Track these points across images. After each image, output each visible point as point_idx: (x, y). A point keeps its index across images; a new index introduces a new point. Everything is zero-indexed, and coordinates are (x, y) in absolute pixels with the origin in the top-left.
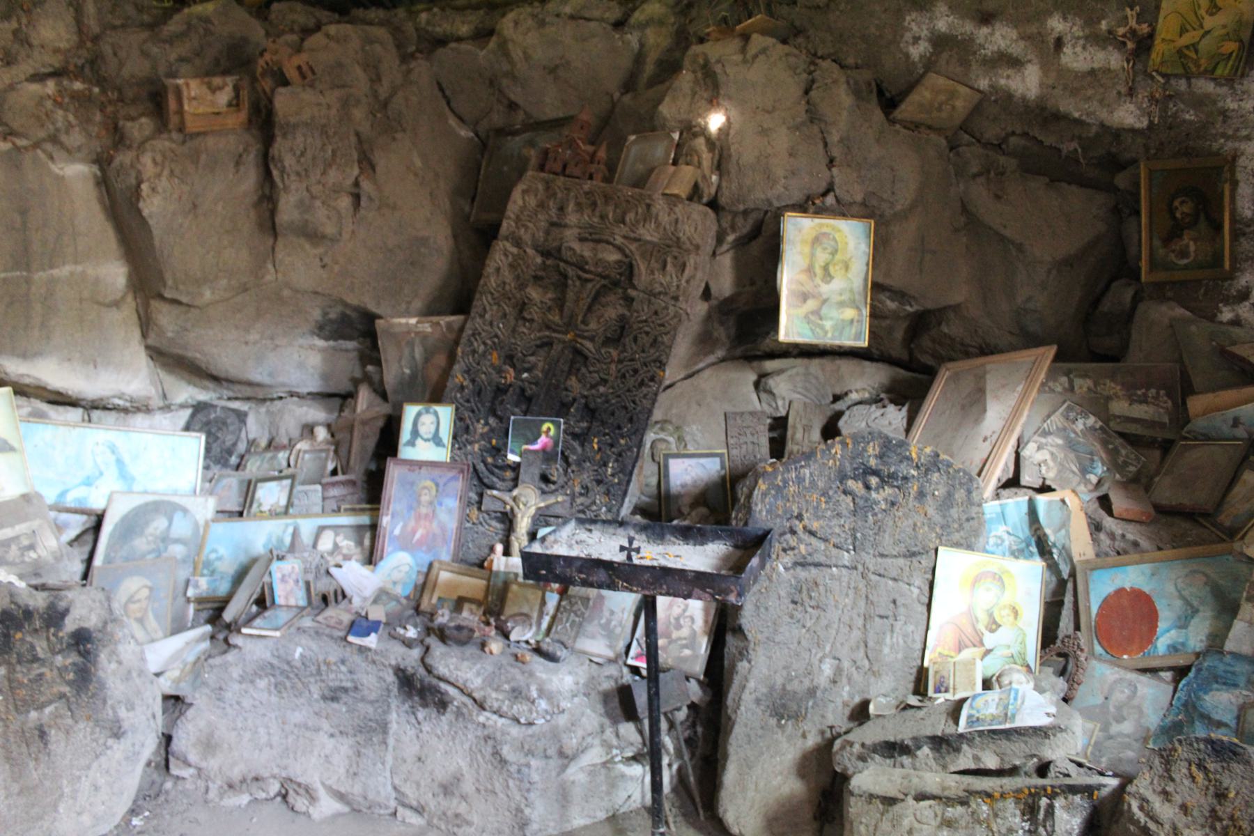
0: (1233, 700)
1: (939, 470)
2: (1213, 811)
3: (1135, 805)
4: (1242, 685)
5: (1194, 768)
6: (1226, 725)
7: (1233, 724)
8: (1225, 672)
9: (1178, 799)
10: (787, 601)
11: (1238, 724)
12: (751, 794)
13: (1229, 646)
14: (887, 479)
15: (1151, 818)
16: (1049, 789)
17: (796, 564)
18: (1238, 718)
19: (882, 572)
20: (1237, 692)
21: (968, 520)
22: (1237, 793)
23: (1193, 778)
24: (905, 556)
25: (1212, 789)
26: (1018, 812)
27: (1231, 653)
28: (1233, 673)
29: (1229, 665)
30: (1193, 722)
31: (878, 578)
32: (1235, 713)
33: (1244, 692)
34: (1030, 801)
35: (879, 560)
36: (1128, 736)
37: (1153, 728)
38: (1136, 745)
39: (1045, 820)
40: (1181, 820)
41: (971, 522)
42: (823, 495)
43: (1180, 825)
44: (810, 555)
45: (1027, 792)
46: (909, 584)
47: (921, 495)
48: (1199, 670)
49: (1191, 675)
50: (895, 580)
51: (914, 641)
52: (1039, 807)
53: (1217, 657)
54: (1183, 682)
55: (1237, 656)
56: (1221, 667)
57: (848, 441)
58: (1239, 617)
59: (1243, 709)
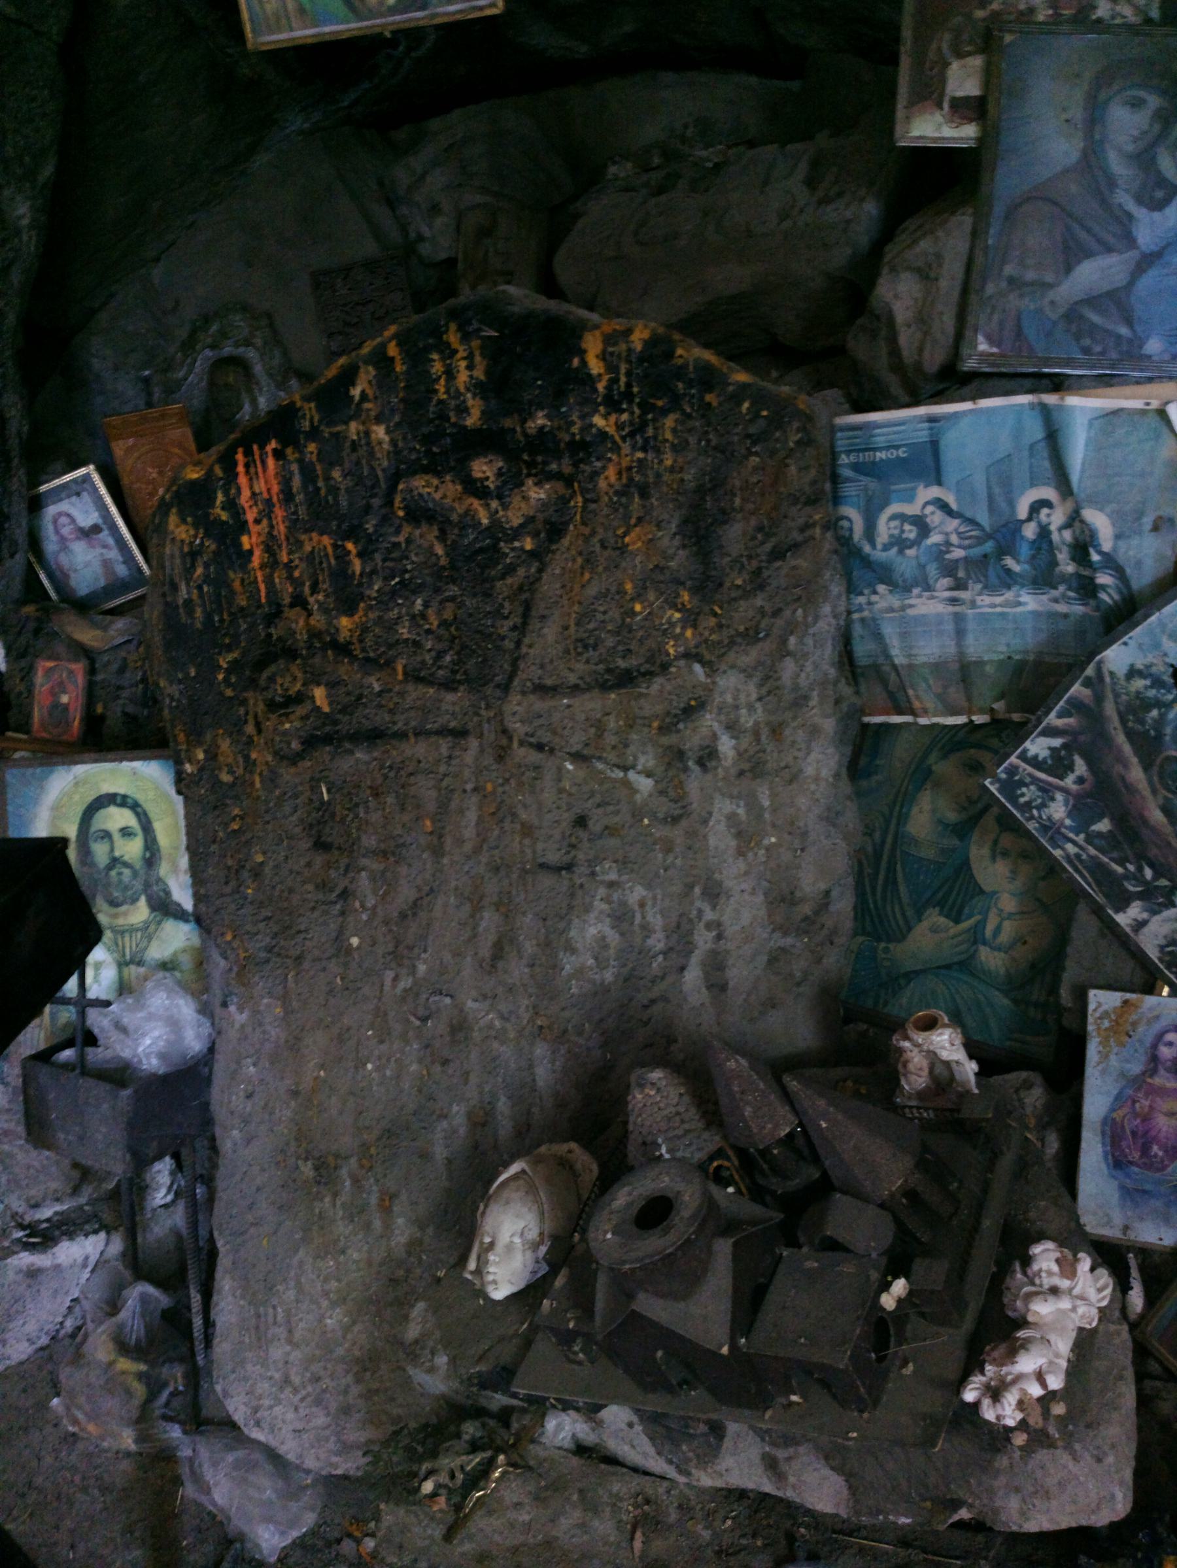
1: (675, 402)
10: (305, 844)
12: (277, 1352)
14: (527, 457)
17: (311, 743)
19: (545, 737)
21: (778, 554)
24: (605, 687)
31: (534, 757)
35: (539, 704)
41: (792, 561)
42: (352, 533)
44: (343, 711)
46: (625, 769)
47: (636, 486)
50: (577, 757)
51: (647, 929)
57: (392, 350)
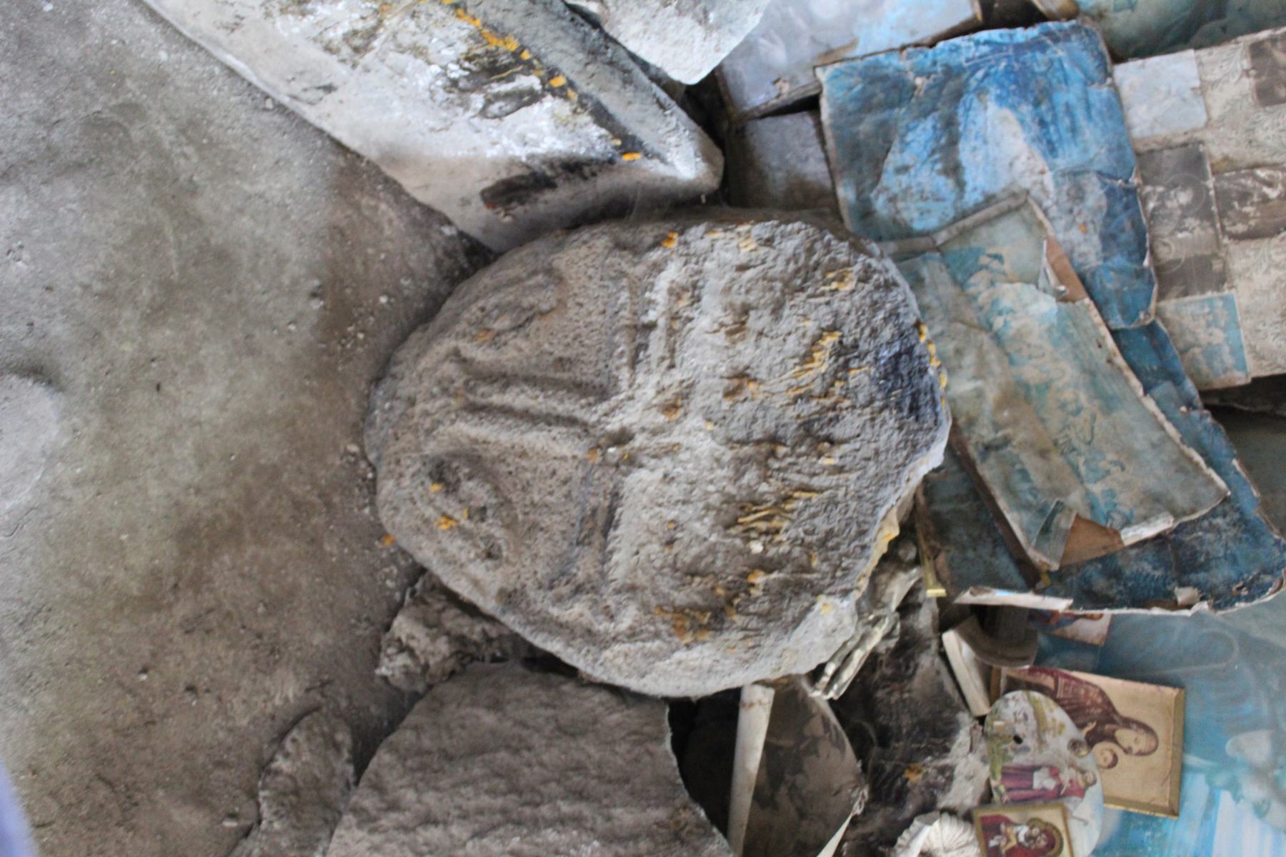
0: (1020, 166)
2: (774, 440)
3: (674, 273)
4: (1062, 162)
5: (829, 341)
6: (961, 185)
7: (972, 198)
8: (1069, 109)
9: (747, 352)
11: (977, 208)
13: (1129, 74)
15: (671, 332)
16: (559, 82)
18: (989, 199)
20: (1040, 163)
22: (840, 470)
23: (807, 357)
25: (813, 406)
26: (462, 48)
27: (1115, 89)
28: (1074, 130)
29: (1088, 107)
30: (925, 114)
32: (997, 188)
33: (1048, 179)
34: (504, 60)
36: (811, 20)
37: (858, 52)
38: (806, 51)
39: (498, 97)
40: (709, 395)
43: (698, 401)
45: (513, 46)
48: (1037, 45)
49: (1021, 34)
52: (510, 79)
53: (1090, 63)
54: (995, 35)
55: (1117, 107)
56: (1069, 95)
58: (1203, 53)
59: (1013, 204)
